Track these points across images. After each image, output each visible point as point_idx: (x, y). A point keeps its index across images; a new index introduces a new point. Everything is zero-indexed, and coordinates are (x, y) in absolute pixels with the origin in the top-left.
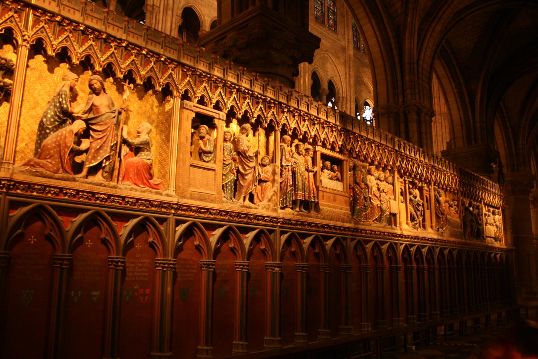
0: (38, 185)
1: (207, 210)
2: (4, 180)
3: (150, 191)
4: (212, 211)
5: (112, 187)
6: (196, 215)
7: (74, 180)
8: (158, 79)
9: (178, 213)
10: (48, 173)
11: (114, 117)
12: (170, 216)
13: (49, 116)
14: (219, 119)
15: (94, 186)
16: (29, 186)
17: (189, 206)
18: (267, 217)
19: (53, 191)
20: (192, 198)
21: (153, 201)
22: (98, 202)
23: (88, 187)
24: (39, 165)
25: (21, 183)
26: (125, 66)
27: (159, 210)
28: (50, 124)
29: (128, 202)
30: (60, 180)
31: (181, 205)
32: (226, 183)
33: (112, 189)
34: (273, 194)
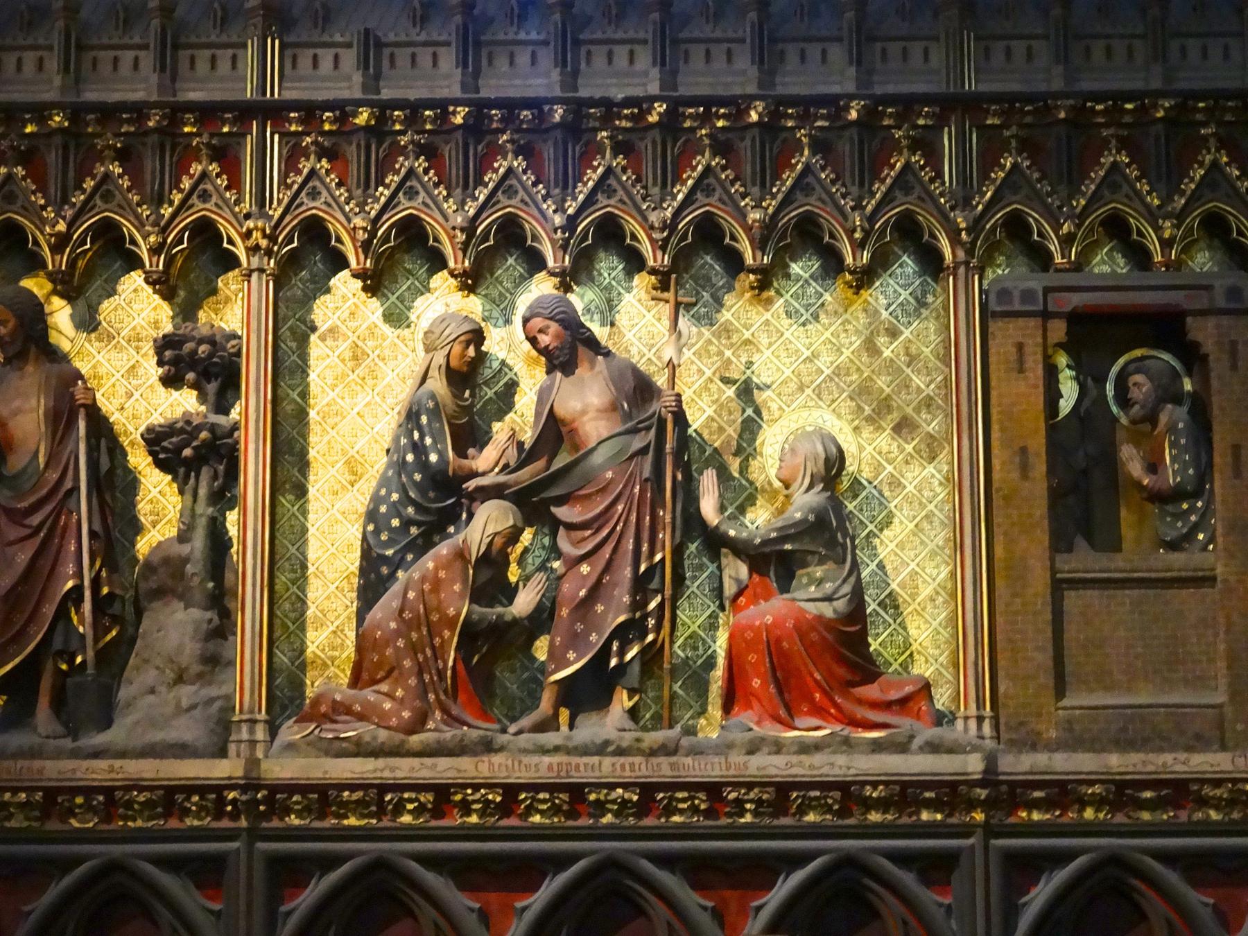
0: (353, 788)
1: (1178, 791)
2: (232, 787)
3: (847, 743)
5: (653, 753)
6: (1120, 818)
7: (488, 747)
8: (845, 217)
9: (1012, 820)
10: (383, 735)
11: (643, 451)
12: (971, 841)
13: (383, 509)
15: (575, 760)
16: (323, 797)
17: (1062, 784)
19: (411, 801)
20: (1074, 741)
21: (863, 784)
22: (608, 819)
23: (550, 767)
24: (348, 711)
25: (292, 788)
26: (669, 213)
27: (905, 820)
28: (390, 543)
29: (739, 802)
31: (1013, 785)
33: (655, 760)
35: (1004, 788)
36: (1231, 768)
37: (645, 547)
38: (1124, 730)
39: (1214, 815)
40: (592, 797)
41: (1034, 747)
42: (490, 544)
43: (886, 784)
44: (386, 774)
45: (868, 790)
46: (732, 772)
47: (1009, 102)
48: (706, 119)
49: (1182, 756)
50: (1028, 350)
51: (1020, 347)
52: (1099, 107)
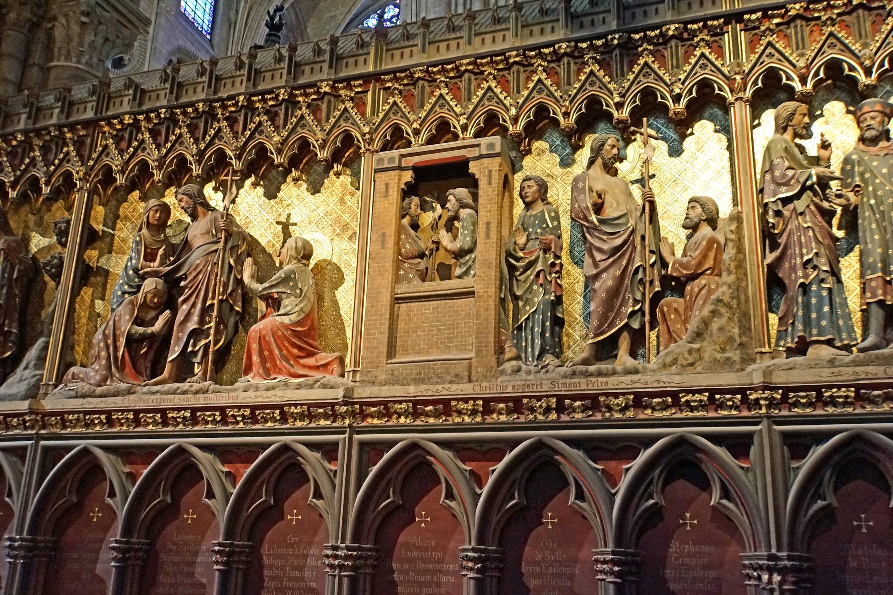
0: (73, 413)
4: (462, 406)
5: (197, 392)
6: (418, 422)
7: (129, 392)
14: (481, 157)
15: (165, 397)
17: (385, 404)
18: (694, 392)
20: (392, 381)
27: (313, 425)
30: (105, 396)
31: (362, 404)
32: (528, 319)
33: (197, 396)
34: (714, 313)
35: (357, 406)
36: (472, 392)
37: (210, 295)
38: (420, 373)
39: (467, 419)
40: (170, 415)
41: (373, 383)
42: (145, 297)
43: (302, 405)
44: (87, 406)
45: (293, 409)
46: (231, 401)
47: (394, 72)
48: (264, 100)
49: (447, 386)
50: (390, 186)
51: (387, 185)
52: (435, 69)
